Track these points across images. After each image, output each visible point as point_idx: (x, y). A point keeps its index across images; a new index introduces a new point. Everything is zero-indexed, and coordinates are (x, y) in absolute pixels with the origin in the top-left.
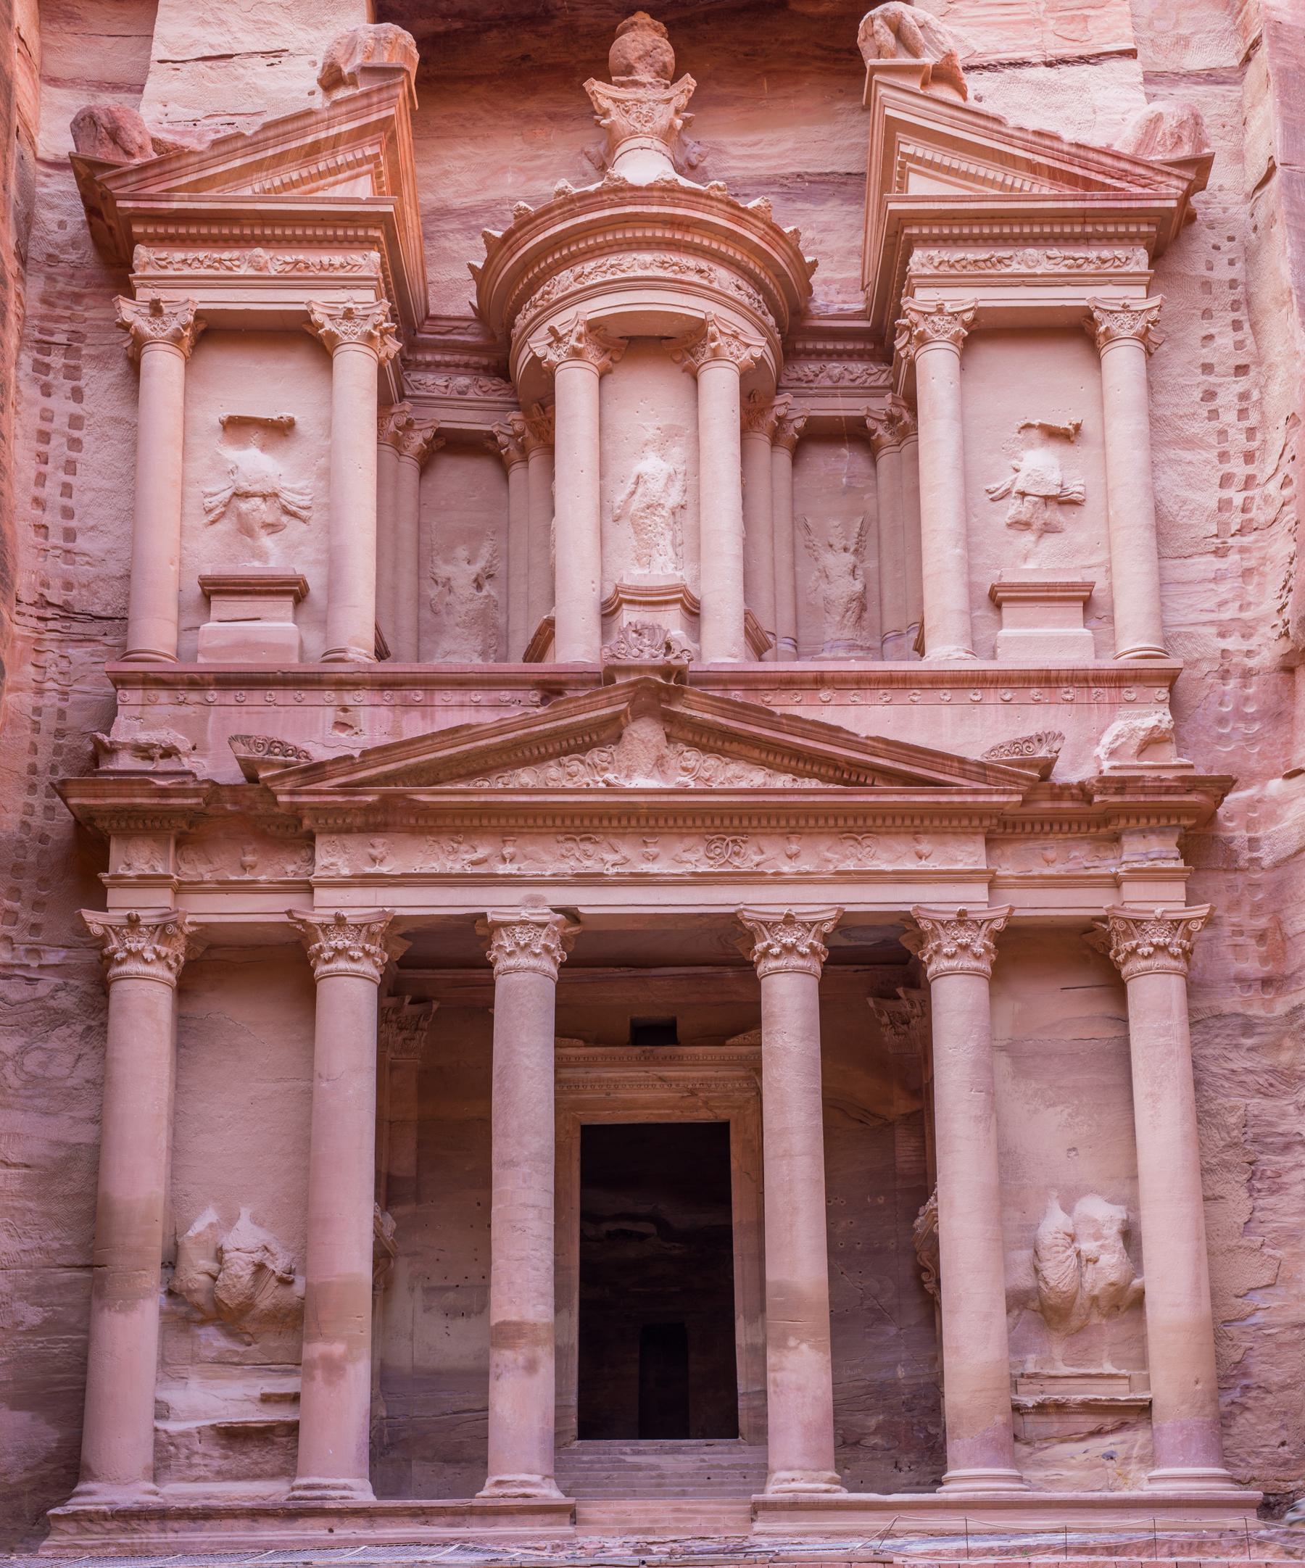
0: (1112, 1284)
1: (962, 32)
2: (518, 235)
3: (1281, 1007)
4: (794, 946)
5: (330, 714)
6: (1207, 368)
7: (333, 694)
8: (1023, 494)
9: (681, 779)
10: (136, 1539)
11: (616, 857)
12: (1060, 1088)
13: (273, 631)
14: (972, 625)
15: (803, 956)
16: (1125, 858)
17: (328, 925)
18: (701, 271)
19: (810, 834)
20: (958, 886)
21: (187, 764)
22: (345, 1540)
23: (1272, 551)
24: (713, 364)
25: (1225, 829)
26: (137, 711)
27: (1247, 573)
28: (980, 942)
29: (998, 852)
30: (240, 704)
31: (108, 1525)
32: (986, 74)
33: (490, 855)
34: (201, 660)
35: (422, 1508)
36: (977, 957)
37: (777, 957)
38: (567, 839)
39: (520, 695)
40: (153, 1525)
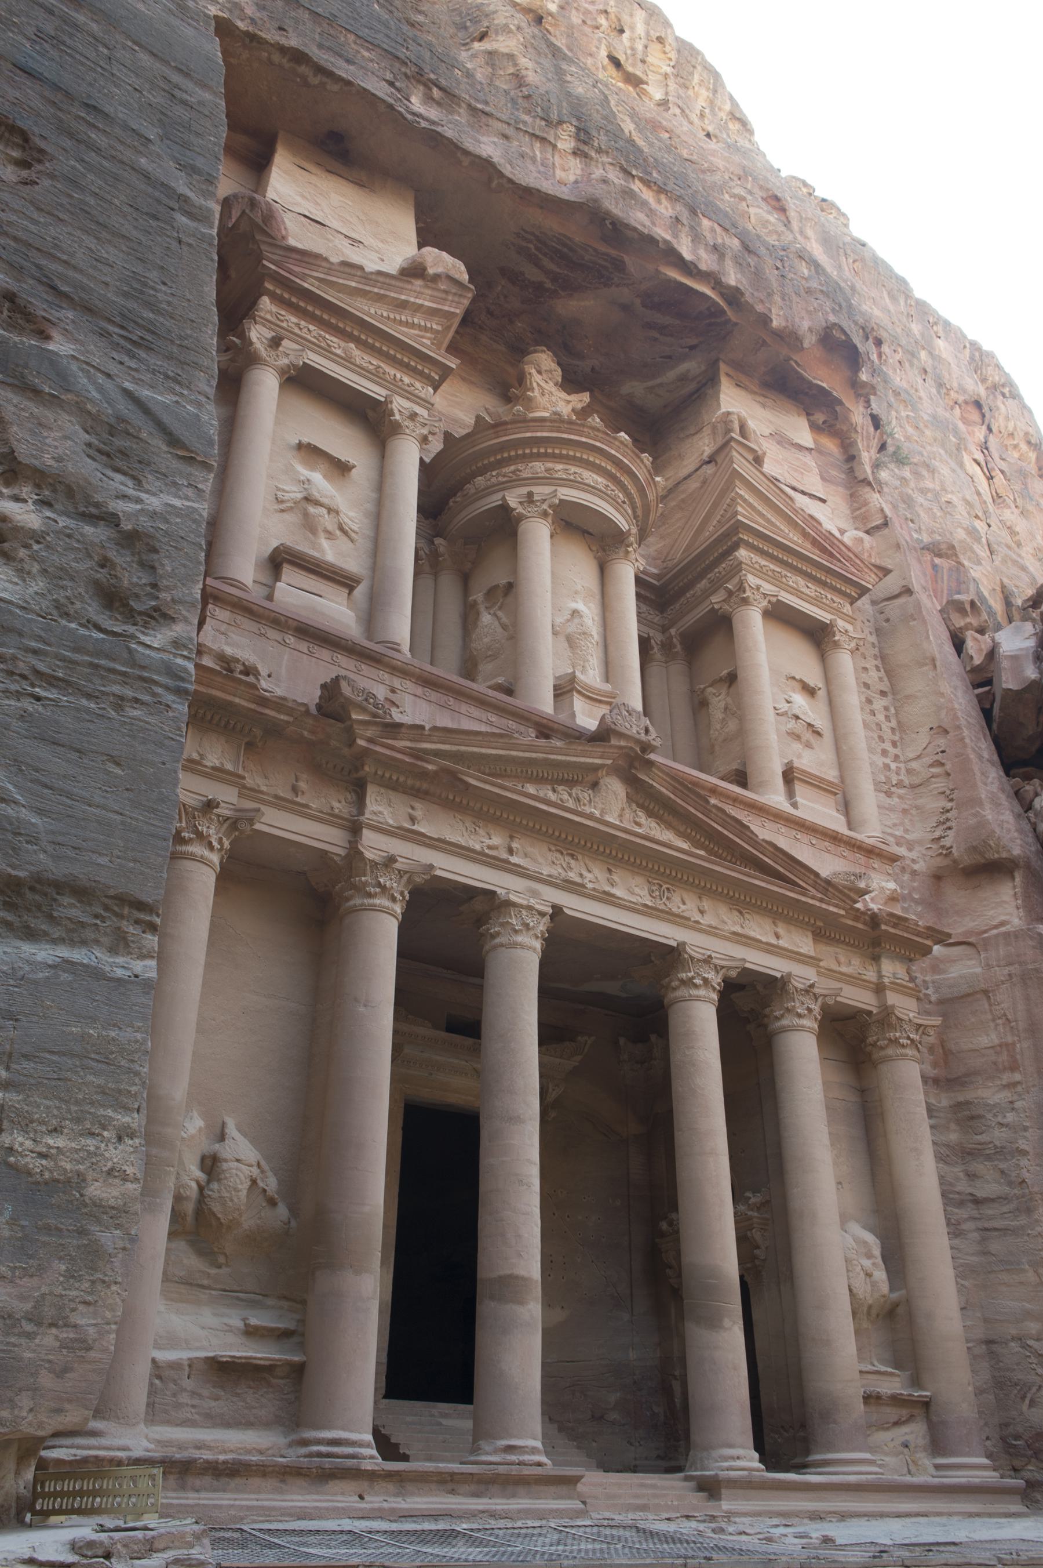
0: (884, 1296)
2: (509, 426)
3: (945, 1101)
6: (867, 686)
7: (386, 675)
8: (797, 718)
13: (337, 611)
15: (714, 989)
17: (376, 864)
18: (624, 502)
20: (801, 965)
22: (380, 1509)
23: (920, 802)
24: (624, 561)
26: (223, 627)
27: (905, 811)
28: (816, 1008)
30: (311, 654)
35: (452, 1475)
38: (557, 850)
39: (522, 728)
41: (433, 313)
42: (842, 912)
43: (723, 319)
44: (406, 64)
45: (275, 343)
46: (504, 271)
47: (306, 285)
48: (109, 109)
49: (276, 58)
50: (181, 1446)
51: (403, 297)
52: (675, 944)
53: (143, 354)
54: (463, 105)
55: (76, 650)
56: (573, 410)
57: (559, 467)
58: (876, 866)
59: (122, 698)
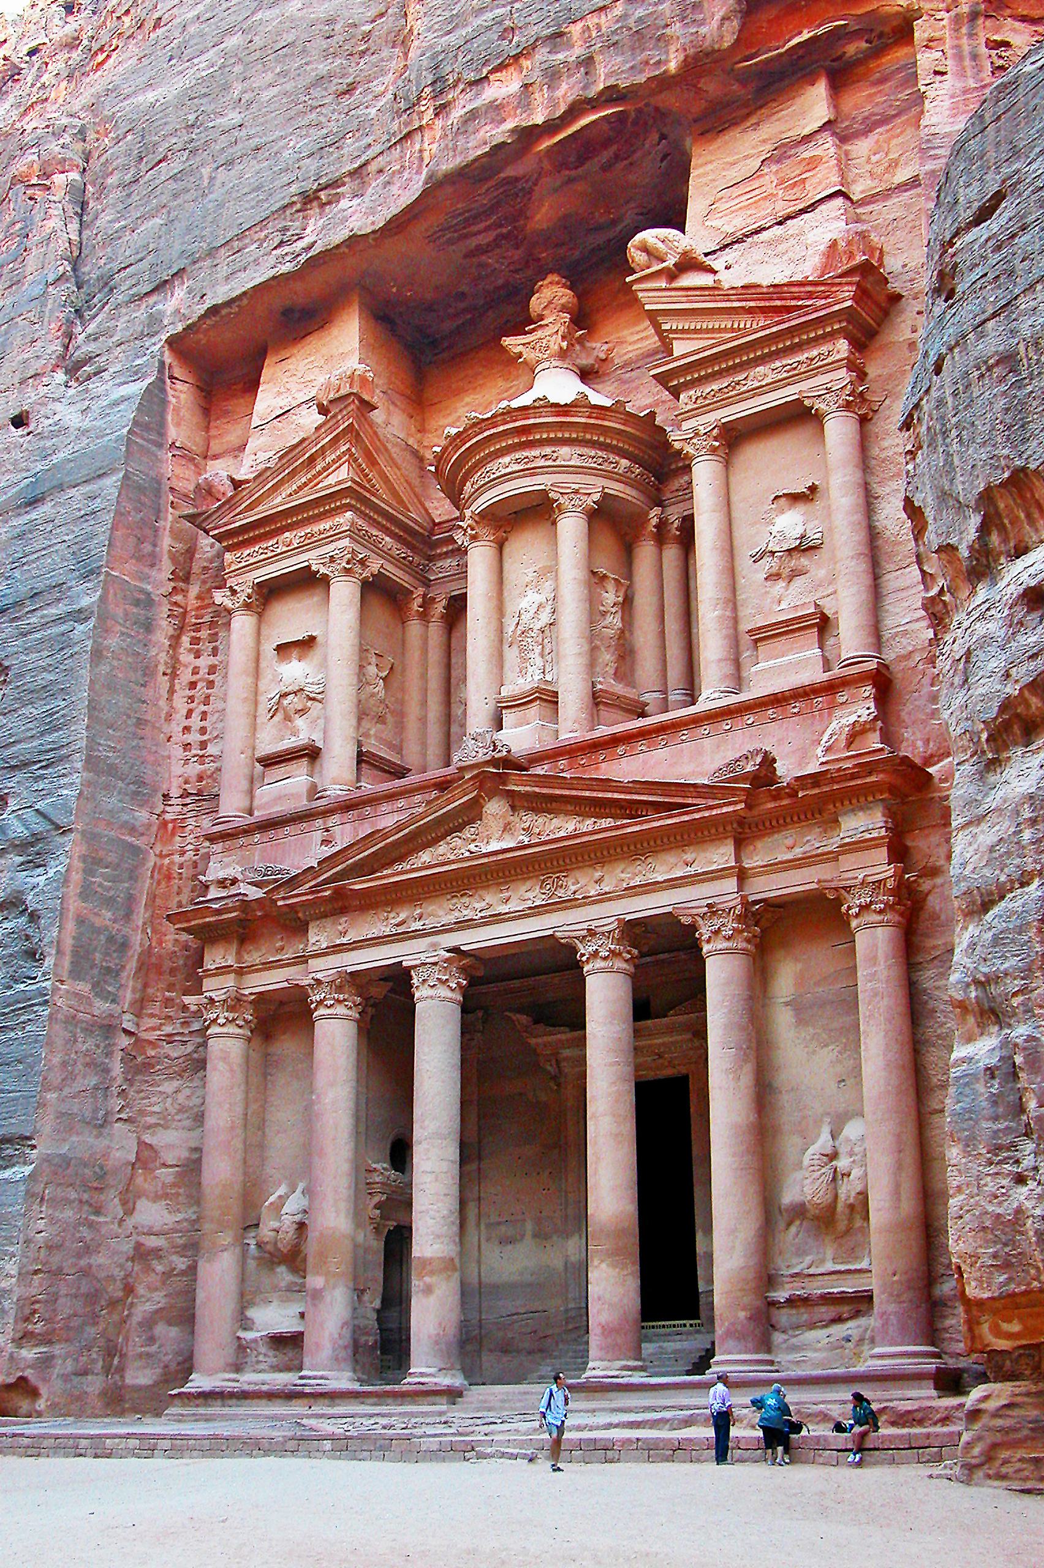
1: (717, 223)
4: (596, 952)
5: (318, 836)
8: (773, 553)
9: (521, 837)
10: (210, 1411)
11: (483, 904)
12: (831, 1030)
14: (737, 664)
15: (605, 958)
16: (842, 836)
19: (610, 861)
21: (243, 888)
25: (940, 790)
28: (730, 925)
29: (751, 848)
31: (198, 1402)
32: (735, 246)
33: (407, 917)
34: (256, 813)
36: (729, 938)
37: (588, 961)
40: (219, 1402)
41: (335, 441)
42: (743, 805)
43: (633, 114)
44: (294, 203)
45: (234, 592)
46: (466, 256)
47: (237, 524)
48: (40, 586)
49: (208, 322)
50: (256, 1384)
51: (307, 455)
52: (550, 932)
53: (50, 770)
54: (346, 180)
55: (9, 1006)
56: (564, 338)
57: (476, 477)
58: (845, 698)
59: (24, 1023)
